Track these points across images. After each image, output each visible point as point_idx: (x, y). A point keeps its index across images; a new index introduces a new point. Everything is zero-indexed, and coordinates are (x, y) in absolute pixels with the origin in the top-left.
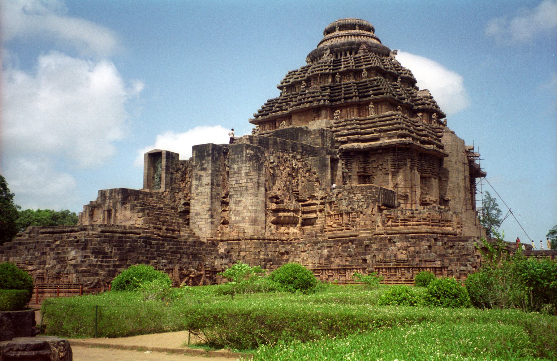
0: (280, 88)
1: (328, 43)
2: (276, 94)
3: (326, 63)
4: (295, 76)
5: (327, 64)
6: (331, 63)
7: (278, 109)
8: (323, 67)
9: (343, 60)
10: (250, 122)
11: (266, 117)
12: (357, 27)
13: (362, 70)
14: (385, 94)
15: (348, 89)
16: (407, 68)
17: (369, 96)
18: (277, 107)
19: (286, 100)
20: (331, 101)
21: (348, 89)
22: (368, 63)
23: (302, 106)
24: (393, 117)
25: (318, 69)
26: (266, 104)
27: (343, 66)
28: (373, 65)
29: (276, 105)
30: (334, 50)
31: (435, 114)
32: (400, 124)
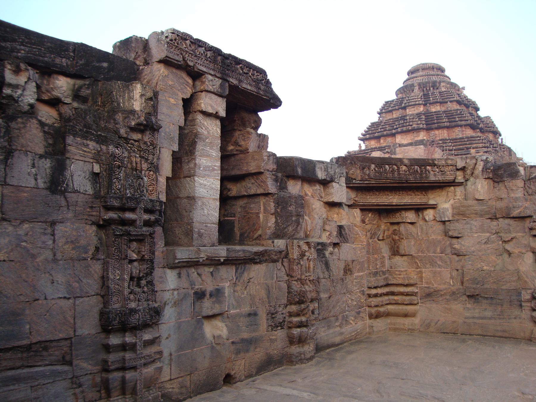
0: (379, 113)
1: (416, 81)
2: (375, 118)
3: (418, 96)
4: (392, 105)
5: (419, 97)
6: (421, 96)
7: (382, 130)
8: (417, 100)
9: (430, 94)
10: (359, 140)
11: (372, 135)
12: (435, 70)
13: (447, 102)
14: (469, 121)
15: (439, 116)
16: (473, 100)
17: (457, 121)
18: (380, 129)
19: (389, 123)
20: (427, 125)
21: (439, 116)
22: (452, 96)
23: (404, 129)
24: (479, 138)
25: (413, 100)
26: (370, 126)
27: (431, 99)
28: (455, 98)
29: (381, 127)
30: (422, 86)
31: (498, 135)
32: (485, 143)
